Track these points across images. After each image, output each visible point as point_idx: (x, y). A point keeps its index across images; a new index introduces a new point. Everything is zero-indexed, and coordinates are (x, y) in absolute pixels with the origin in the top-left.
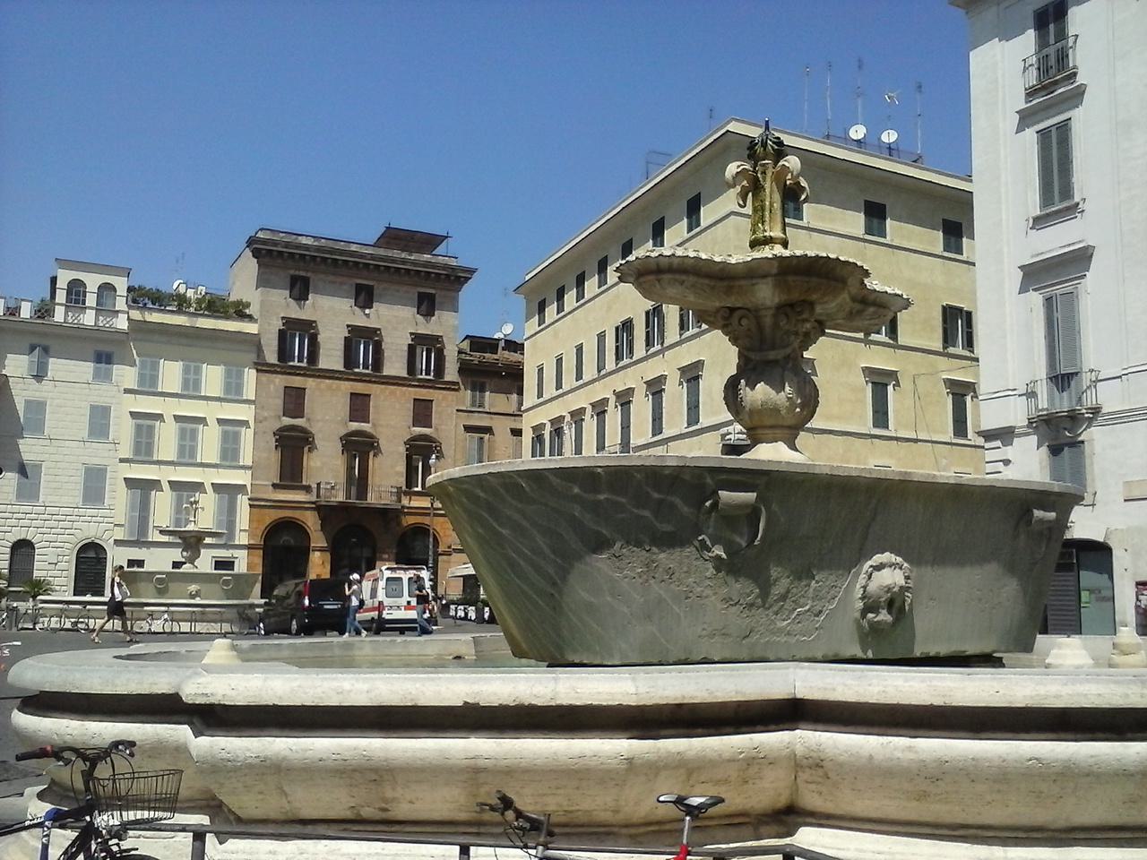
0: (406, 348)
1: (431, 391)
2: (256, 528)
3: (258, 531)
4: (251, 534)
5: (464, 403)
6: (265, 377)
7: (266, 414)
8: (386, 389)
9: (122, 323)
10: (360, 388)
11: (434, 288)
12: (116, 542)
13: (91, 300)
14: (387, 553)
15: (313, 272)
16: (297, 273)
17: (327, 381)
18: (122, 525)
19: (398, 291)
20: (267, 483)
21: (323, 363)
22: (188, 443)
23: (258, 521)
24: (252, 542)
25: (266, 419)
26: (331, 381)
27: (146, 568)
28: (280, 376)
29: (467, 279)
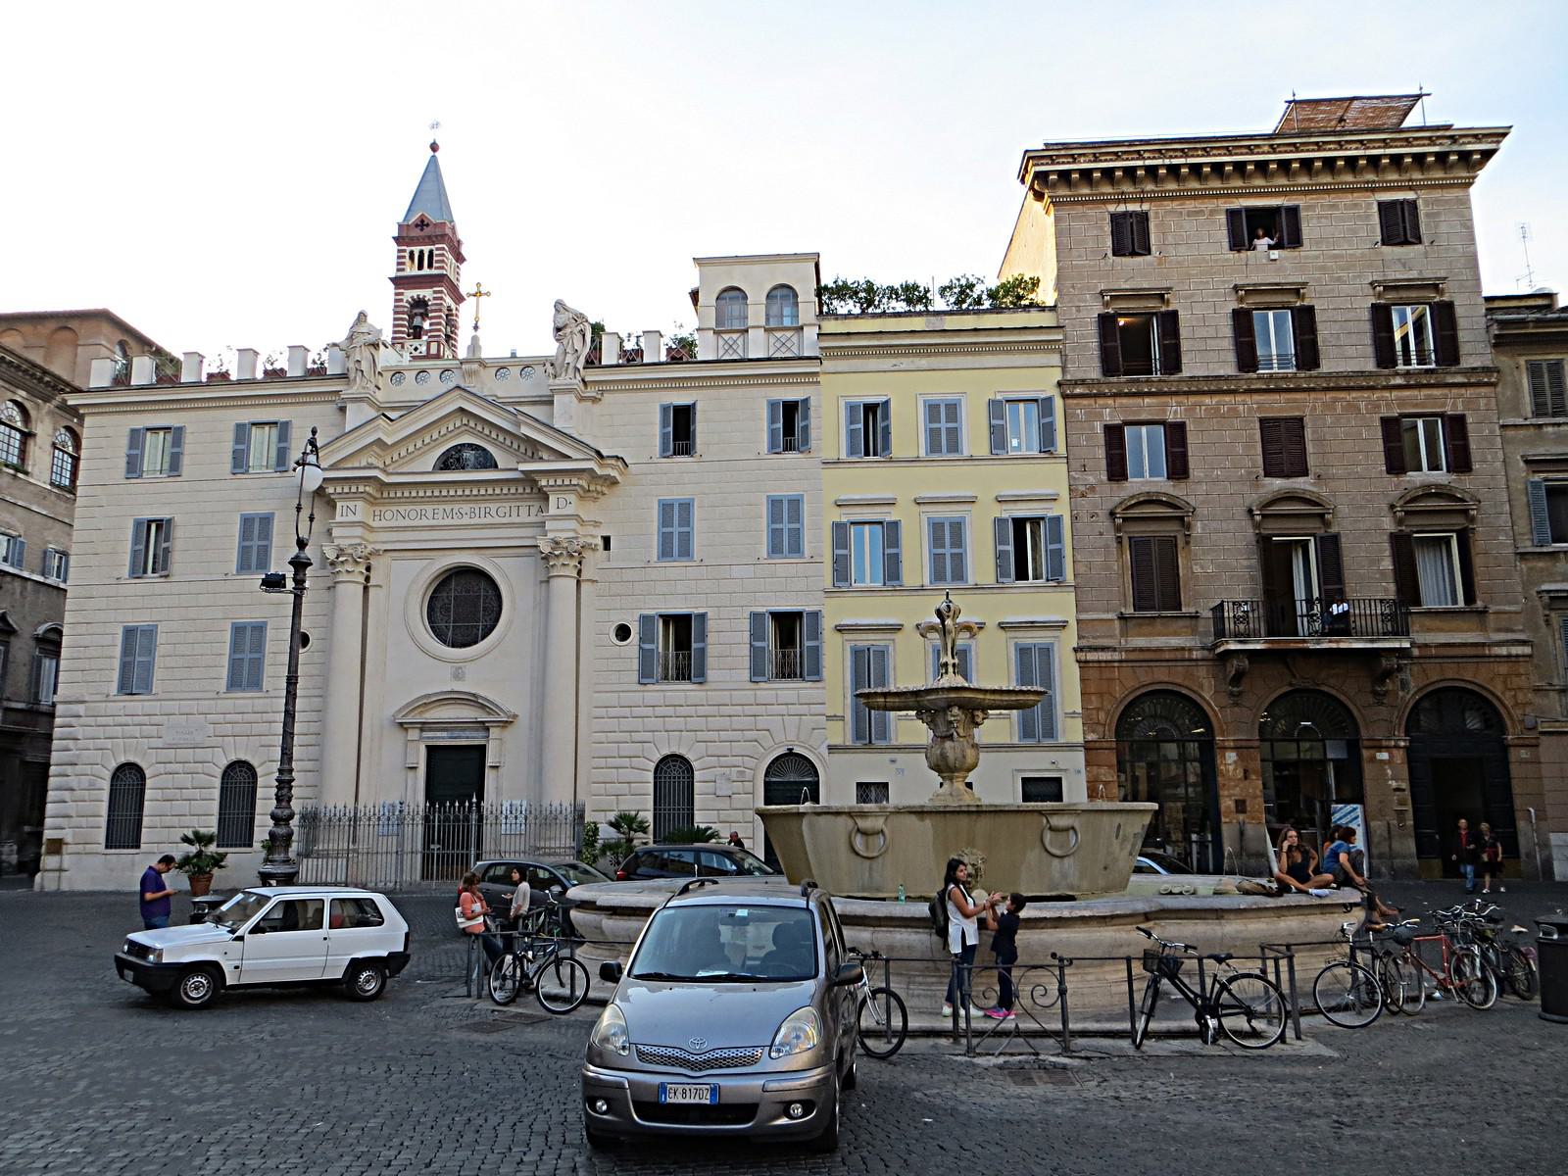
0: (1366, 315)
1: (1437, 392)
2: (1098, 709)
3: (1102, 716)
4: (1089, 724)
5: (1516, 410)
6: (1065, 212)
7: (1091, 480)
8: (1335, 400)
9: (810, 342)
10: (1279, 406)
11: (1410, 188)
12: (832, 749)
13: (756, 313)
14: (1387, 748)
15: (1150, 200)
16: (1122, 208)
17: (1207, 400)
18: (842, 718)
19: (1334, 207)
20: (1110, 616)
21: (1192, 366)
22: (948, 551)
23: (1100, 694)
24: (1091, 737)
25: (1092, 488)
26: (1216, 399)
27: (895, 799)
28: (1110, 401)
29: (1488, 155)
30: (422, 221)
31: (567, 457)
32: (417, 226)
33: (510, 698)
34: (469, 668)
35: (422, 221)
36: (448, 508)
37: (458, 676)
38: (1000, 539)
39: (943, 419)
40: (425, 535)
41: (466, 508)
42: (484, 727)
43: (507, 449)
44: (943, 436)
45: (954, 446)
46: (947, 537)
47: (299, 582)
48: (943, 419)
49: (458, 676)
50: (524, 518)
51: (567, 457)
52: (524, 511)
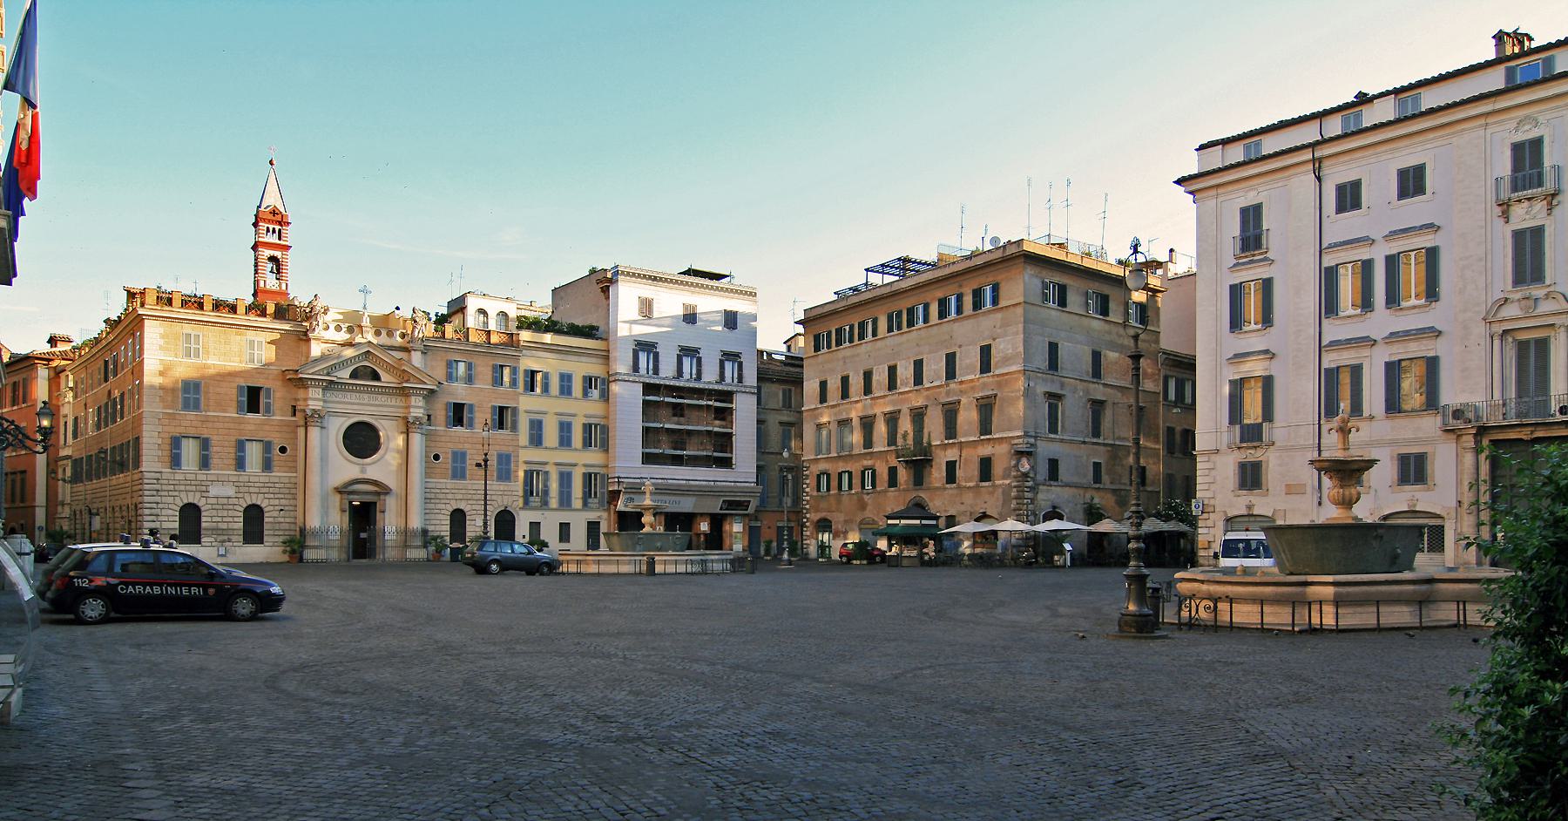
30: (274, 211)
31: (425, 383)
32: (271, 213)
33: (391, 481)
34: (369, 469)
35: (274, 211)
36: (358, 395)
37: (363, 471)
38: (584, 432)
39: (566, 379)
40: (349, 407)
41: (366, 396)
42: (378, 494)
43: (387, 372)
44: (566, 390)
45: (569, 393)
46: (565, 429)
47: (486, 465)
48: (566, 379)
49: (363, 471)
50: (393, 403)
51: (425, 383)
52: (394, 400)
